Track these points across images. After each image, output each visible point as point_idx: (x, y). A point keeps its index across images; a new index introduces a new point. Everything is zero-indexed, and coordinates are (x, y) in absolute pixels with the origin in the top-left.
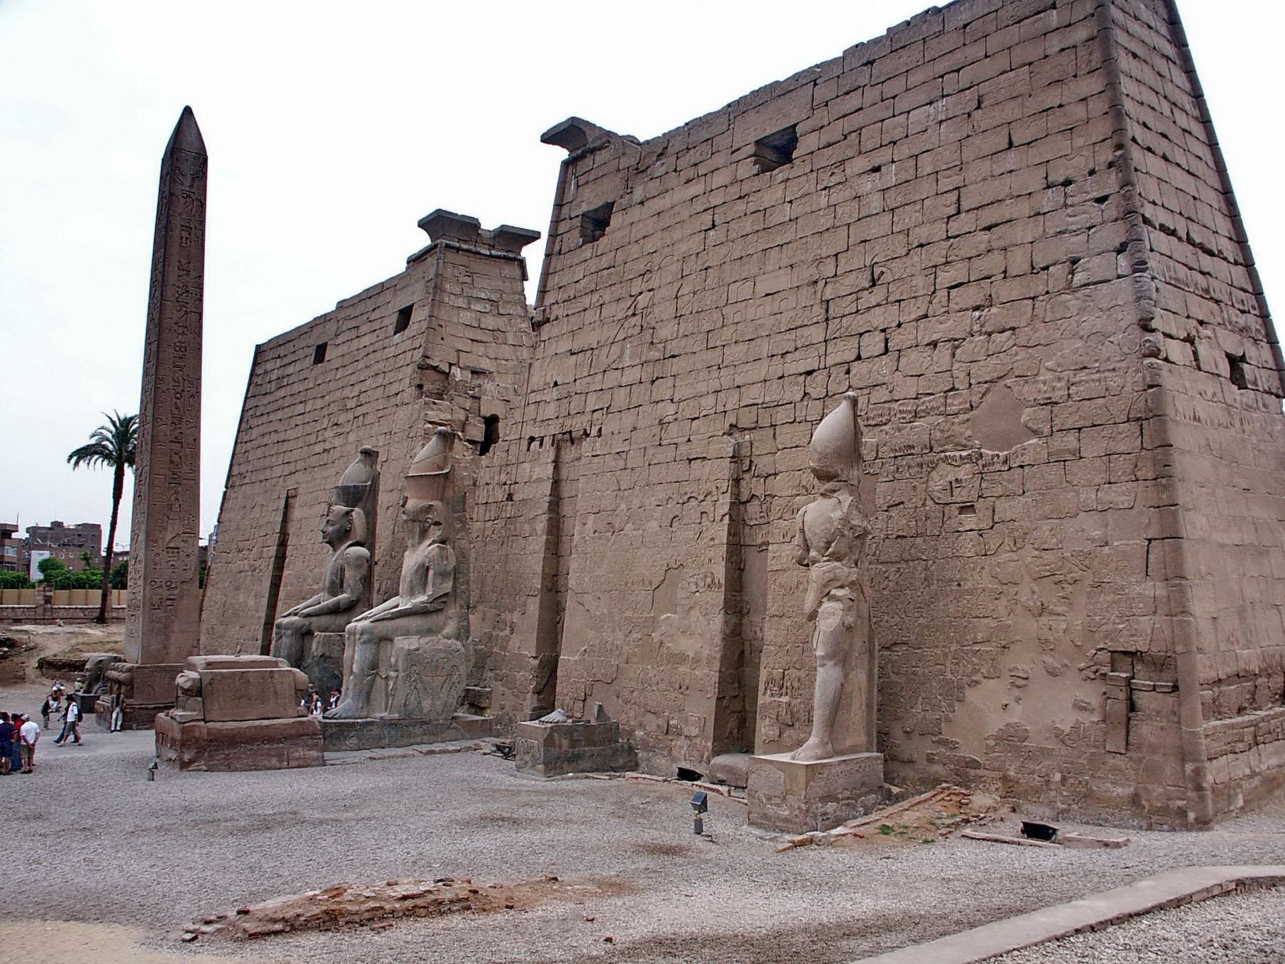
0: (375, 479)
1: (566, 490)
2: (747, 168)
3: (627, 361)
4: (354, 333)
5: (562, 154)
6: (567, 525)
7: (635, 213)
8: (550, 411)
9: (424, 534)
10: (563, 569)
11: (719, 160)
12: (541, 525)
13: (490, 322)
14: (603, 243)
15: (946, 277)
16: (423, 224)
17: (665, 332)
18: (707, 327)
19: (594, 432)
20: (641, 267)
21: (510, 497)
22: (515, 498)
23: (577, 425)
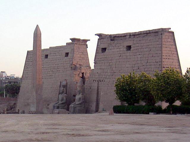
0: (67, 83)
1: (99, 88)
2: (125, 49)
3: (108, 72)
4: (55, 55)
5: (98, 37)
6: (100, 93)
7: (110, 51)
8: (97, 77)
9: (80, 94)
10: (99, 99)
11: (121, 47)
12: (96, 92)
13: (82, 56)
14: (105, 53)
15: (146, 70)
16: (71, 39)
17: (114, 69)
18: (119, 70)
19: (104, 81)
20: (111, 59)
21: (91, 88)
22: (92, 88)
23: (101, 79)
